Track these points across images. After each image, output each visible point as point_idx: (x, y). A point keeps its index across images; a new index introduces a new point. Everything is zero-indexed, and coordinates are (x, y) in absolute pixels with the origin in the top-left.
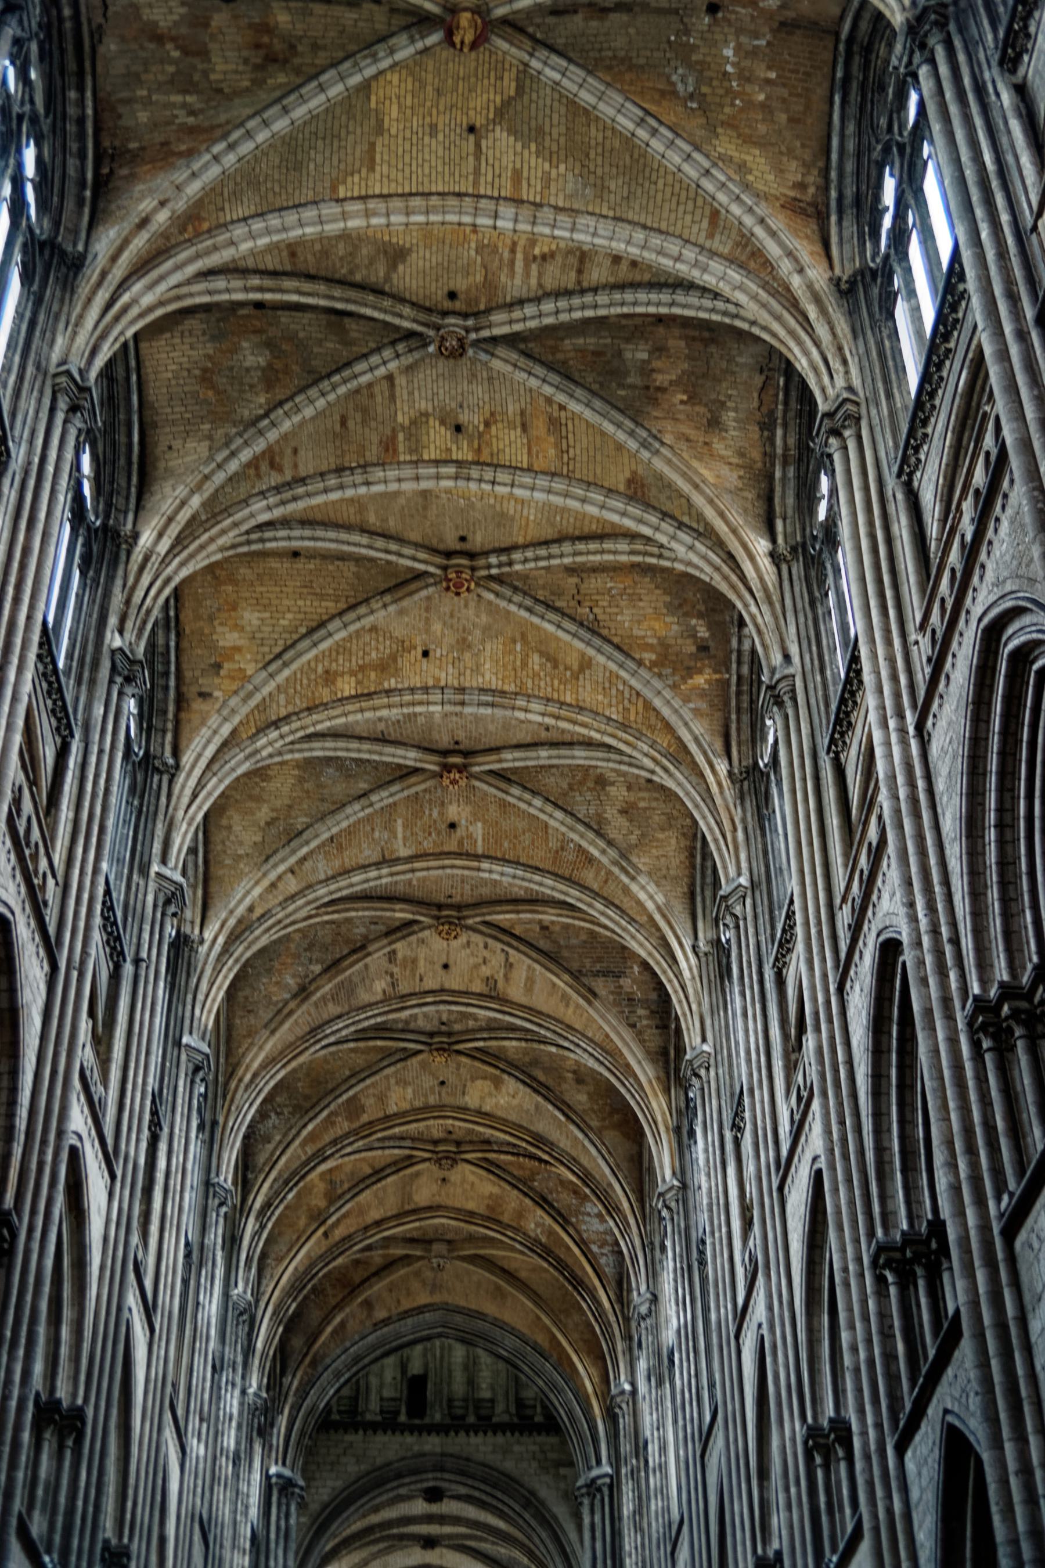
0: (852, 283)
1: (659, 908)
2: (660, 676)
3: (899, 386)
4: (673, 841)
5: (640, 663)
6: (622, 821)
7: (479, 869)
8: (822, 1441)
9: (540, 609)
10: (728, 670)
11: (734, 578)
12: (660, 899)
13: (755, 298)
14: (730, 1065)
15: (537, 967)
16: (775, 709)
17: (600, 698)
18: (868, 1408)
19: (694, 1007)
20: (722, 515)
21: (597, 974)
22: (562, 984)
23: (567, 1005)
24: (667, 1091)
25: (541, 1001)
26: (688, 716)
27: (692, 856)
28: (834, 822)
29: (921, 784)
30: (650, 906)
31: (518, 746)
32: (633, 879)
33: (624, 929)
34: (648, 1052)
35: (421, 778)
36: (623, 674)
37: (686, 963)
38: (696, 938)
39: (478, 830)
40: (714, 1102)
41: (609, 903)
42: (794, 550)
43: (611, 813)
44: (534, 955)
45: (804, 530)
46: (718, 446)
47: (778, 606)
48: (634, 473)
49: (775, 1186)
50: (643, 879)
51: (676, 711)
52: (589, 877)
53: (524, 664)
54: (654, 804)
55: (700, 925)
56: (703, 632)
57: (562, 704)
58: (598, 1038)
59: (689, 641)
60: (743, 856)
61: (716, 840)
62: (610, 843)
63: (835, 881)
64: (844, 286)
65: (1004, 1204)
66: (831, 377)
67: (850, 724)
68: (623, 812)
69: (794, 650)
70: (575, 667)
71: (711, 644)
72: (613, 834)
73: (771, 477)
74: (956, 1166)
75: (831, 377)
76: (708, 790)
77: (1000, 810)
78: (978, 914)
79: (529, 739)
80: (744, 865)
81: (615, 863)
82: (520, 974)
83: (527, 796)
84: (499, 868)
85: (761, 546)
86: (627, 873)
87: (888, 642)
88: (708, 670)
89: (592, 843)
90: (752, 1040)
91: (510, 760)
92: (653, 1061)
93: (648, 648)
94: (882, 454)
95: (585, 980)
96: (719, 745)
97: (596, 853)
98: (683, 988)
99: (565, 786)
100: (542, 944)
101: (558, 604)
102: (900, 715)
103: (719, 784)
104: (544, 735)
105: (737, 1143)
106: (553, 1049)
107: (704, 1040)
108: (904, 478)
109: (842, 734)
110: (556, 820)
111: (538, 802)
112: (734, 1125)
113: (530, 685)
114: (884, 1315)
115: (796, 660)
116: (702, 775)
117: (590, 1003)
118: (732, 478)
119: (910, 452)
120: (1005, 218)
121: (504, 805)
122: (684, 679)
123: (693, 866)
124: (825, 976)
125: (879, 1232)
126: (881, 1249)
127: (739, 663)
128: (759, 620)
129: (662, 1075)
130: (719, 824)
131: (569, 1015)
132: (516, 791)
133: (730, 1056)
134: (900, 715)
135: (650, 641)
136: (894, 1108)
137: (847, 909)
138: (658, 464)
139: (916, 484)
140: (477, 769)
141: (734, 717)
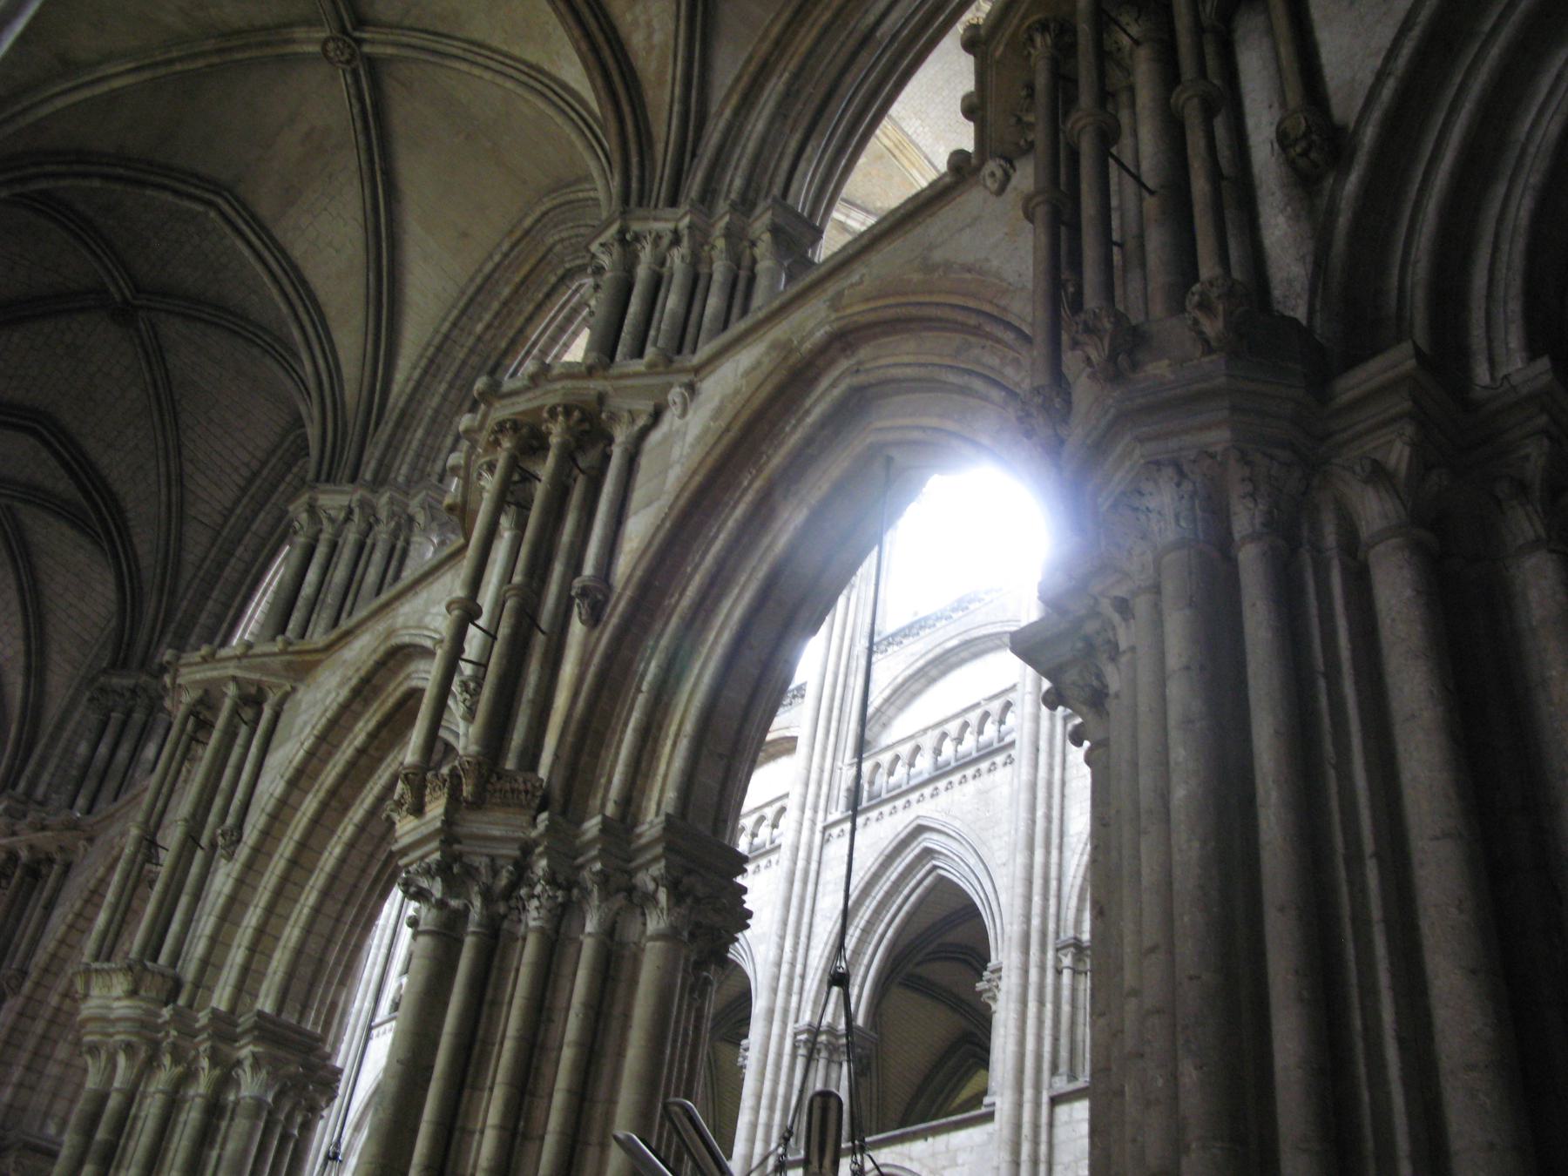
29: (814, 866)
87: (823, 757)
94: (859, 621)
119: (885, 643)
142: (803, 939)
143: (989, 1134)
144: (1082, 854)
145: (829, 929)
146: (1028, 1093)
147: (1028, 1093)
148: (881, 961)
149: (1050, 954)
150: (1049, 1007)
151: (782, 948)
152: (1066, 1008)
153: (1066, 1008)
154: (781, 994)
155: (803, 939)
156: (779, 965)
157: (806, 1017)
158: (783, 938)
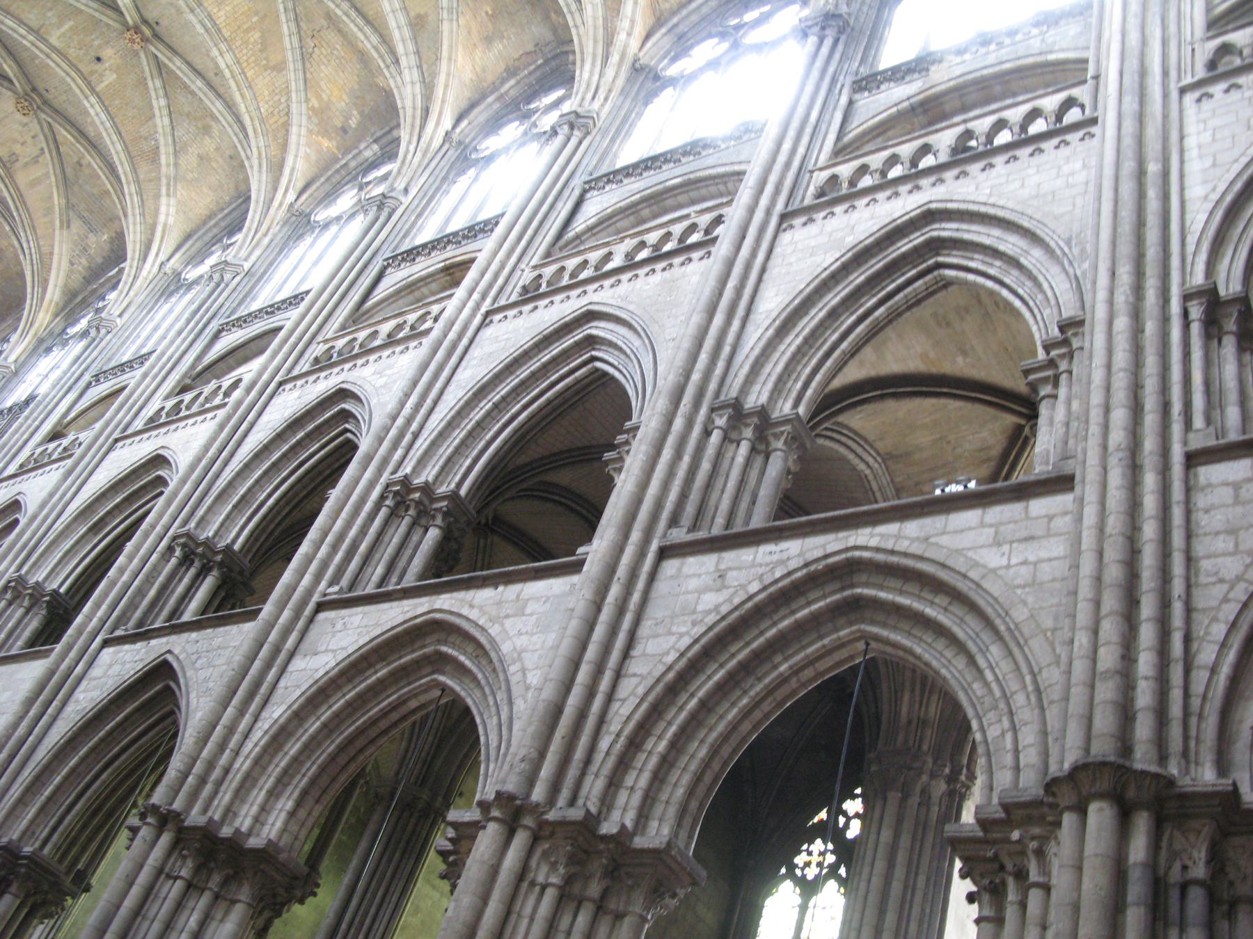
0: (642, 68)
1: (165, 225)
2: (309, 118)
3: (622, 142)
4: (209, 200)
5: (307, 100)
6: (194, 161)
7: (87, 98)
8: (20, 588)
9: (292, 16)
10: (344, 154)
11: (418, 122)
12: (171, 221)
13: (595, 18)
14: (124, 343)
15: (53, 179)
16: (375, 208)
17: (266, 93)
18: (104, 607)
19: (132, 293)
20: (446, 86)
21: (81, 217)
22: (56, 202)
23: (45, 215)
24: (56, 315)
25: (32, 197)
26: (301, 153)
27: (210, 217)
28: (355, 296)
29: (465, 341)
30: (162, 218)
31: (188, 64)
32: (168, 195)
33: (134, 215)
34: (65, 285)
35: (118, 18)
36: (294, 95)
37: (150, 268)
38: (168, 260)
39: (111, 78)
40: (95, 353)
41: (140, 193)
42: (460, 143)
43: (194, 150)
44: (58, 171)
45: (474, 139)
46: (478, 53)
47: (426, 161)
48: (426, 15)
49: (115, 435)
50: (173, 201)
51: (299, 144)
52: (144, 169)
53: (247, 31)
54: (220, 171)
55: (177, 256)
56: (353, 123)
57: (244, 73)
58: (45, 250)
59: (341, 118)
60: (257, 253)
61: (249, 229)
62: (176, 165)
63: (327, 326)
64: (637, 65)
65: (330, 590)
66: (593, 98)
67: (414, 260)
68: (200, 157)
69: (413, 191)
70: (271, 64)
71: (350, 132)
72: (182, 161)
73: (483, 97)
74: (318, 548)
75: (593, 98)
76: (272, 200)
77: (504, 398)
78: (442, 435)
79: (199, 67)
80: (253, 258)
81: (168, 178)
82: (36, 172)
83: (161, 93)
84: (99, 109)
85: (447, 124)
86: (168, 189)
87: (509, 255)
88: (334, 143)
89: (167, 154)
90: (172, 350)
91: (176, 65)
92: (64, 293)
93: (319, 98)
94: (585, 162)
95: (71, 213)
96: (300, 185)
97: (163, 160)
98: (135, 278)
99: (186, 110)
100: (69, 170)
101: (302, 24)
102: (484, 297)
103: (281, 204)
104: (210, 75)
105: (89, 385)
106: (8, 228)
107: (120, 316)
108: (587, 187)
109: (403, 260)
110: (162, 122)
111: (163, 102)
112: (96, 376)
113: (238, 44)
114: (156, 570)
115: (410, 197)
116: (275, 189)
117: (61, 227)
118: (468, 75)
120: (801, 150)
121: (142, 82)
122: (318, 133)
123: (205, 223)
124: (278, 370)
125: (192, 524)
126: (188, 535)
127: (354, 157)
128: (409, 157)
129: (61, 304)
130: (260, 224)
131: (41, 222)
132: (158, 83)
133: (128, 338)
134: (484, 297)
135: (324, 96)
136: (260, 472)
137: (322, 348)
138: (446, 27)
139: (588, 195)
140: (153, 49)
141: (323, 179)
142: (429, 402)
143: (573, 585)
144: (767, 329)
145: (459, 396)
146: (636, 536)
147: (636, 536)
148: (506, 442)
149: (703, 411)
150: (687, 459)
151: (402, 404)
152: (706, 466)
153: (706, 466)
154: (386, 444)
155: (429, 402)
156: (394, 418)
157: (407, 469)
158: (407, 396)
